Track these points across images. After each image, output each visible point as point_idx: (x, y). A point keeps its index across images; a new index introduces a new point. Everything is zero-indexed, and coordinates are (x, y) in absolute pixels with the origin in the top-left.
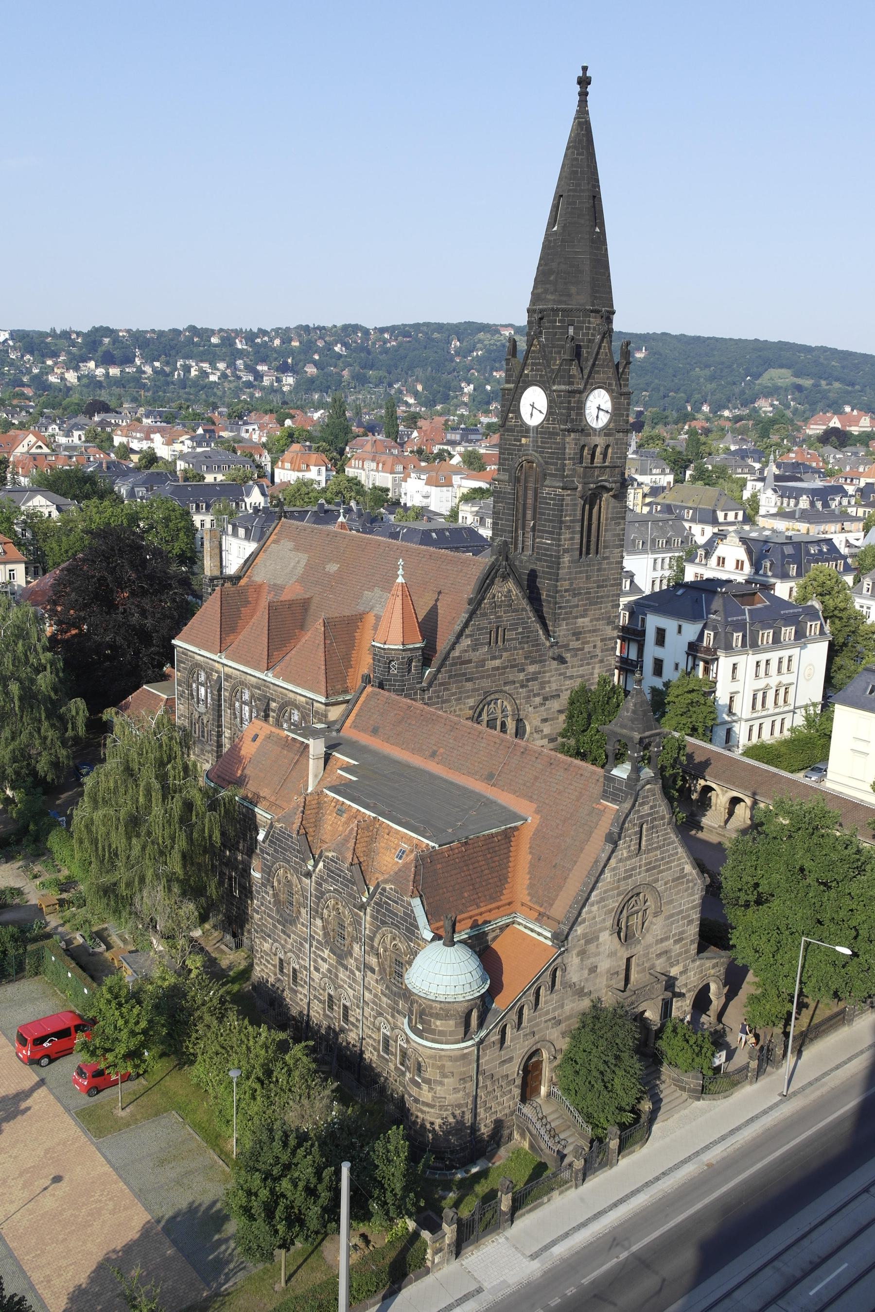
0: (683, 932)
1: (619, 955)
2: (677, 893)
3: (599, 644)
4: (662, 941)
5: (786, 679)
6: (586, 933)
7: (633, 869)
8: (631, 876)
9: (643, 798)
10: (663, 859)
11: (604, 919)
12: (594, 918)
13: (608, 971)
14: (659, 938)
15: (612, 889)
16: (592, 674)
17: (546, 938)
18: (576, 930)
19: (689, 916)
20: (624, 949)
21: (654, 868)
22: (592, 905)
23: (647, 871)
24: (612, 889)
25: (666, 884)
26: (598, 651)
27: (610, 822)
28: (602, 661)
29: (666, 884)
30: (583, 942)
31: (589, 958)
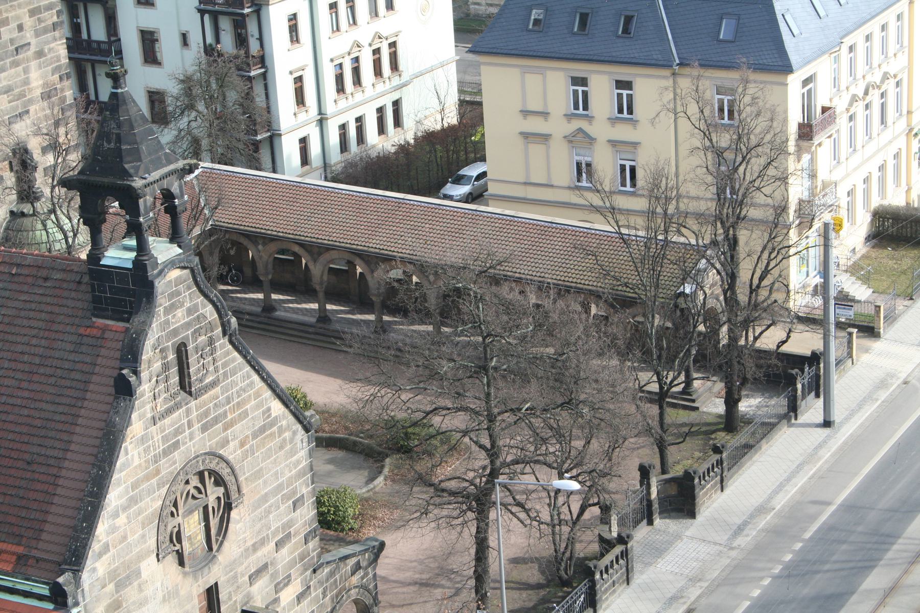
0: (289, 524)
1: (183, 592)
2: (268, 455)
3: (28, 22)
4: (255, 548)
6: (115, 570)
7: (178, 432)
8: (176, 445)
9: (172, 296)
11: (143, 536)
12: (125, 538)
14: (250, 543)
15: (147, 478)
16: (26, 82)
17: (40, 597)
19: (294, 492)
20: (190, 579)
21: (216, 420)
22: (116, 515)
23: (204, 429)
24: (147, 478)
25: (242, 444)
26: (29, 36)
27: (118, 355)
28: (40, 54)
29: (242, 444)
30: (111, 587)
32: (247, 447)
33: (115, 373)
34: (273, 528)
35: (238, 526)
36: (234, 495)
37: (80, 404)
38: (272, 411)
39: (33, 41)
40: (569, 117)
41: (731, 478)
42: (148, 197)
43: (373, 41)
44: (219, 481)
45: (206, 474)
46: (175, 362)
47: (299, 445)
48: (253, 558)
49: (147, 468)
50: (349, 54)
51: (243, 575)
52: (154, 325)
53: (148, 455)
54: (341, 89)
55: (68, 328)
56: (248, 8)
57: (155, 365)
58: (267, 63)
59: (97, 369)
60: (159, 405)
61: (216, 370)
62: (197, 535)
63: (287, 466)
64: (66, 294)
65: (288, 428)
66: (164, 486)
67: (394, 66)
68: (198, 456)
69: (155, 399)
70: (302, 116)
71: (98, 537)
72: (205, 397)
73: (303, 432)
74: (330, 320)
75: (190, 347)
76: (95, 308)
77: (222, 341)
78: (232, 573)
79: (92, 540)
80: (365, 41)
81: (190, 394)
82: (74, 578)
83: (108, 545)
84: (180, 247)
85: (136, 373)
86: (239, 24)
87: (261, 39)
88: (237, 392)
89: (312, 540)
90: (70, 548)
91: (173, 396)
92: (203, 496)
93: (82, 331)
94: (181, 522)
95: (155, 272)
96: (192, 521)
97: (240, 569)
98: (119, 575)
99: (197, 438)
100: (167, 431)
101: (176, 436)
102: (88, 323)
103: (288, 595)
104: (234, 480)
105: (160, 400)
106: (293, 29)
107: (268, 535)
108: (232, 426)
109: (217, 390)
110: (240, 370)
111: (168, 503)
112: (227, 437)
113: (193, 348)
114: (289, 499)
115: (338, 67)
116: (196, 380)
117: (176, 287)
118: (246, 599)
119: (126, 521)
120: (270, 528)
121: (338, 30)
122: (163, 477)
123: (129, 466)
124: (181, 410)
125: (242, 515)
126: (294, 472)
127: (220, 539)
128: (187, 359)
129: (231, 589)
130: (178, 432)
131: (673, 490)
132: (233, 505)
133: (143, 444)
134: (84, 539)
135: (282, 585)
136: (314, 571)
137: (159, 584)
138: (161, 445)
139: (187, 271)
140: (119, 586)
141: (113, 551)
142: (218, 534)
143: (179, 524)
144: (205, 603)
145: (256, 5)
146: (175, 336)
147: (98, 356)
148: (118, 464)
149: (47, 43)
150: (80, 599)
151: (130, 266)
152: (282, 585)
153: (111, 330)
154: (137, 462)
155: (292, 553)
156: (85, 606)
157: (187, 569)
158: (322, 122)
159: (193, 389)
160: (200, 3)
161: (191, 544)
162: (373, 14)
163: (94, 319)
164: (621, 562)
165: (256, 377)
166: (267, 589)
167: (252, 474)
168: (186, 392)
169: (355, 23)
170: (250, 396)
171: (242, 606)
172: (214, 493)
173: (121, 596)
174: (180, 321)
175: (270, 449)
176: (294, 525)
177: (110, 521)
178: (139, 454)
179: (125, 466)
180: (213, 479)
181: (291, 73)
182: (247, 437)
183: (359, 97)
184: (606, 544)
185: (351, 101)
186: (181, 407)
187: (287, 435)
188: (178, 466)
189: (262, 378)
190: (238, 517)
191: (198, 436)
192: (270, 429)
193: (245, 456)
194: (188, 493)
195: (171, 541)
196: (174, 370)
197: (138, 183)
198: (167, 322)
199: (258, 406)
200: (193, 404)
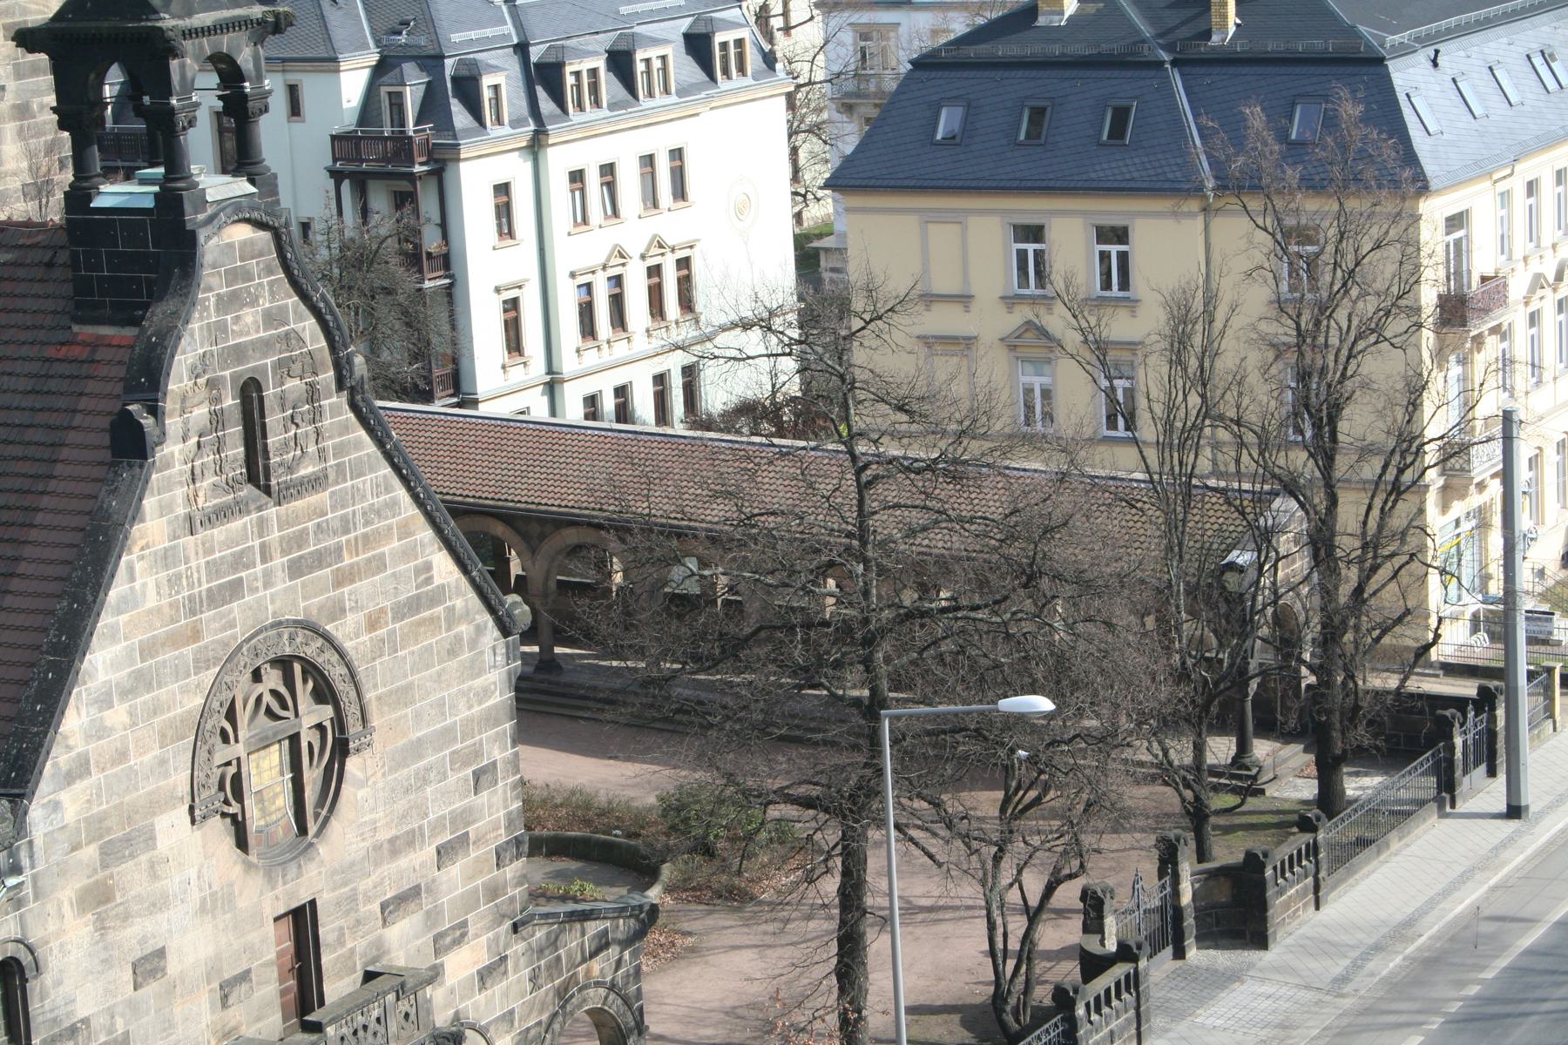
0: (464, 817)
1: (242, 903)
4: (396, 847)
5: (674, 225)
6: (102, 818)
7: (240, 561)
8: (235, 589)
9: (233, 276)
10: (346, 525)
11: (163, 762)
12: (122, 755)
13: (211, 972)
14: (384, 835)
15: (175, 640)
18: (56, 806)
19: (477, 752)
20: (257, 881)
21: (319, 560)
22: (105, 702)
23: (295, 569)
24: (175, 640)
29: (373, 624)
30: (90, 852)
31: (126, 917)
32: (382, 632)
33: (116, 406)
34: (431, 816)
35: (361, 793)
36: (353, 728)
37: (41, 487)
38: (435, 572)
39: (11, 85)
40: (1010, 301)
41: (1334, 888)
42: (188, 61)
43: (648, 249)
44: (324, 693)
45: (297, 668)
46: (237, 415)
47: (488, 657)
48: (390, 869)
49: (173, 621)
50: (604, 268)
51: (368, 900)
52: (195, 325)
53: (178, 593)
54: (588, 328)
55: (25, 351)
56: (421, 164)
57: (197, 412)
58: (455, 269)
59: (78, 420)
60: (201, 494)
61: (322, 455)
62: (276, 796)
63: (463, 693)
64: (22, 288)
65: (467, 616)
66: (208, 668)
67: (687, 303)
68: (277, 624)
69: (194, 481)
70: (517, 375)
71: (66, 738)
72: (298, 504)
73: (497, 633)
74: (559, 667)
75: (270, 392)
76: (78, 305)
77: (334, 399)
78: (347, 889)
79: (53, 740)
80: (634, 248)
81: (267, 490)
82: (14, 811)
83: (88, 762)
84: (252, 182)
85: (154, 411)
86: (404, 199)
87: (444, 225)
88: (364, 514)
89: (511, 861)
90: (8, 753)
91: (231, 486)
92: (290, 714)
93: (50, 352)
94: (243, 756)
95: (201, 217)
96: (265, 764)
97: (364, 885)
98: (109, 830)
99: (280, 587)
100: (217, 555)
101: (236, 570)
102: (61, 336)
103: (461, 964)
104: (353, 694)
105: (205, 484)
106: (504, 212)
107: (421, 828)
108: (352, 581)
109: (321, 498)
110: (372, 470)
111: (216, 705)
112: (341, 600)
113: (275, 395)
114: (466, 764)
115: (584, 289)
116: (281, 464)
117: (242, 260)
118: (375, 953)
119: (126, 720)
120: (427, 815)
121: (585, 221)
122: (206, 647)
123: (136, 606)
124: (247, 519)
125: (369, 773)
126: (476, 709)
127: (324, 812)
128: (263, 416)
129: (342, 922)
130: (240, 561)
131: (1223, 894)
132: (351, 745)
133: (167, 567)
134: (37, 734)
135: (448, 940)
136: (515, 928)
137: (192, 873)
138: (204, 579)
139: (265, 236)
140: (111, 854)
141: (96, 777)
142: (320, 803)
143: (238, 759)
144: (289, 944)
145: (436, 161)
146: (240, 361)
147: (81, 394)
148: (114, 594)
149: (38, 93)
150: (25, 862)
151: (149, 203)
152: (448, 940)
153: (109, 345)
154: (152, 601)
155: (471, 878)
156: (35, 878)
157: (253, 858)
158: (552, 387)
159: (273, 482)
160: (335, 160)
161: (263, 811)
162: (649, 204)
163: (76, 328)
164: (1125, 996)
165: (402, 493)
166: (419, 942)
167: (391, 693)
168: (258, 487)
169: (616, 213)
170: (390, 528)
171: (367, 964)
172: (311, 715)
173: (112, 877)
174: (248, 333)
175: (429, 649)
176: (474, 821)
177: (93, 710)
178: (158, 586)
179: (126, 603)
180: (310, 684)
181: (498, 290)
182: (382, 611)
183: (621, 350)
184: (1093, 965)
185: (607, 356)
186: (249, 513)
187: (464, 629)
188: (239, 633)
189: (415, 497)
190: (360, 775)
191: (282, 584)
192: (430, 607)
193: (378, 649)
194: (259, 699)
195: (221, 787)
196: (235, 431)
197: (168, 22)
198: (222, 328)
199: (408, 554)
200: (272, 512)
